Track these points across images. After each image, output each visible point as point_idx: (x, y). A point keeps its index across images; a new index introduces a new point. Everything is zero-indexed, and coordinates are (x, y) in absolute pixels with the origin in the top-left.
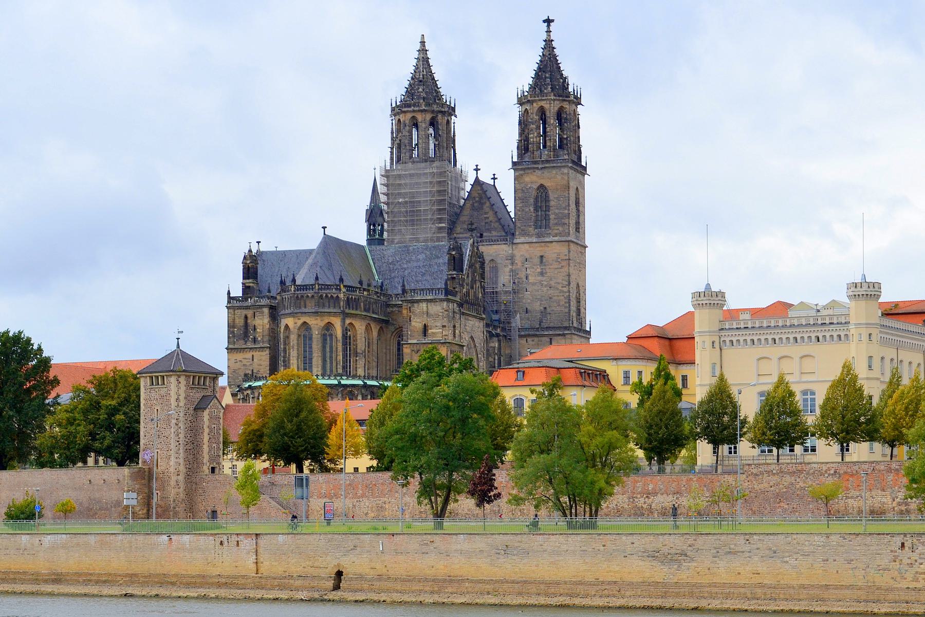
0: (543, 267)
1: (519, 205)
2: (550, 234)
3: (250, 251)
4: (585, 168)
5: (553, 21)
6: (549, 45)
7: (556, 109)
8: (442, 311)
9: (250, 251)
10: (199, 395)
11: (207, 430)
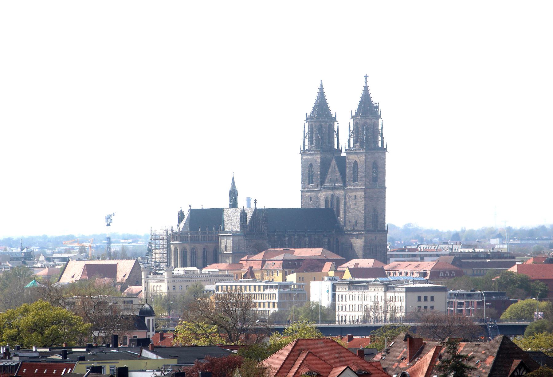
3: (181, 211)
6: (366, 89)
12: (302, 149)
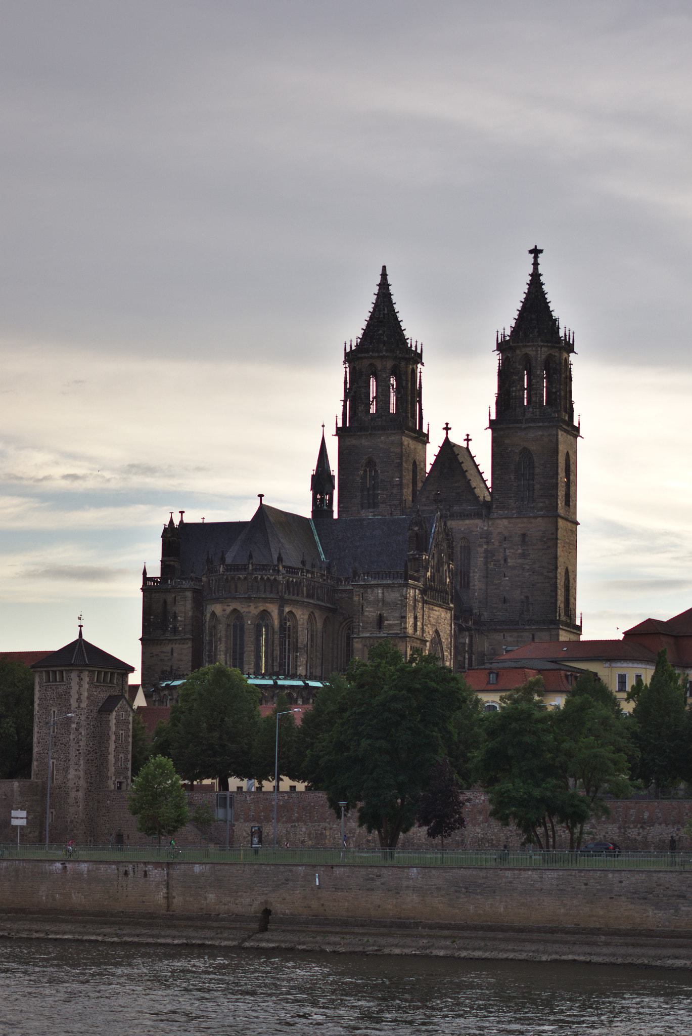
0: (526, 548)
1: (497, 472)
2: (534, 507)
3: (171, 522)
4: (577, 429)
5: (541, 251)
7: (543, 357)
8: (400, 598)
9: (171, 522)
10: (104, 695)
11: (113, 737)
12: (340, 425)
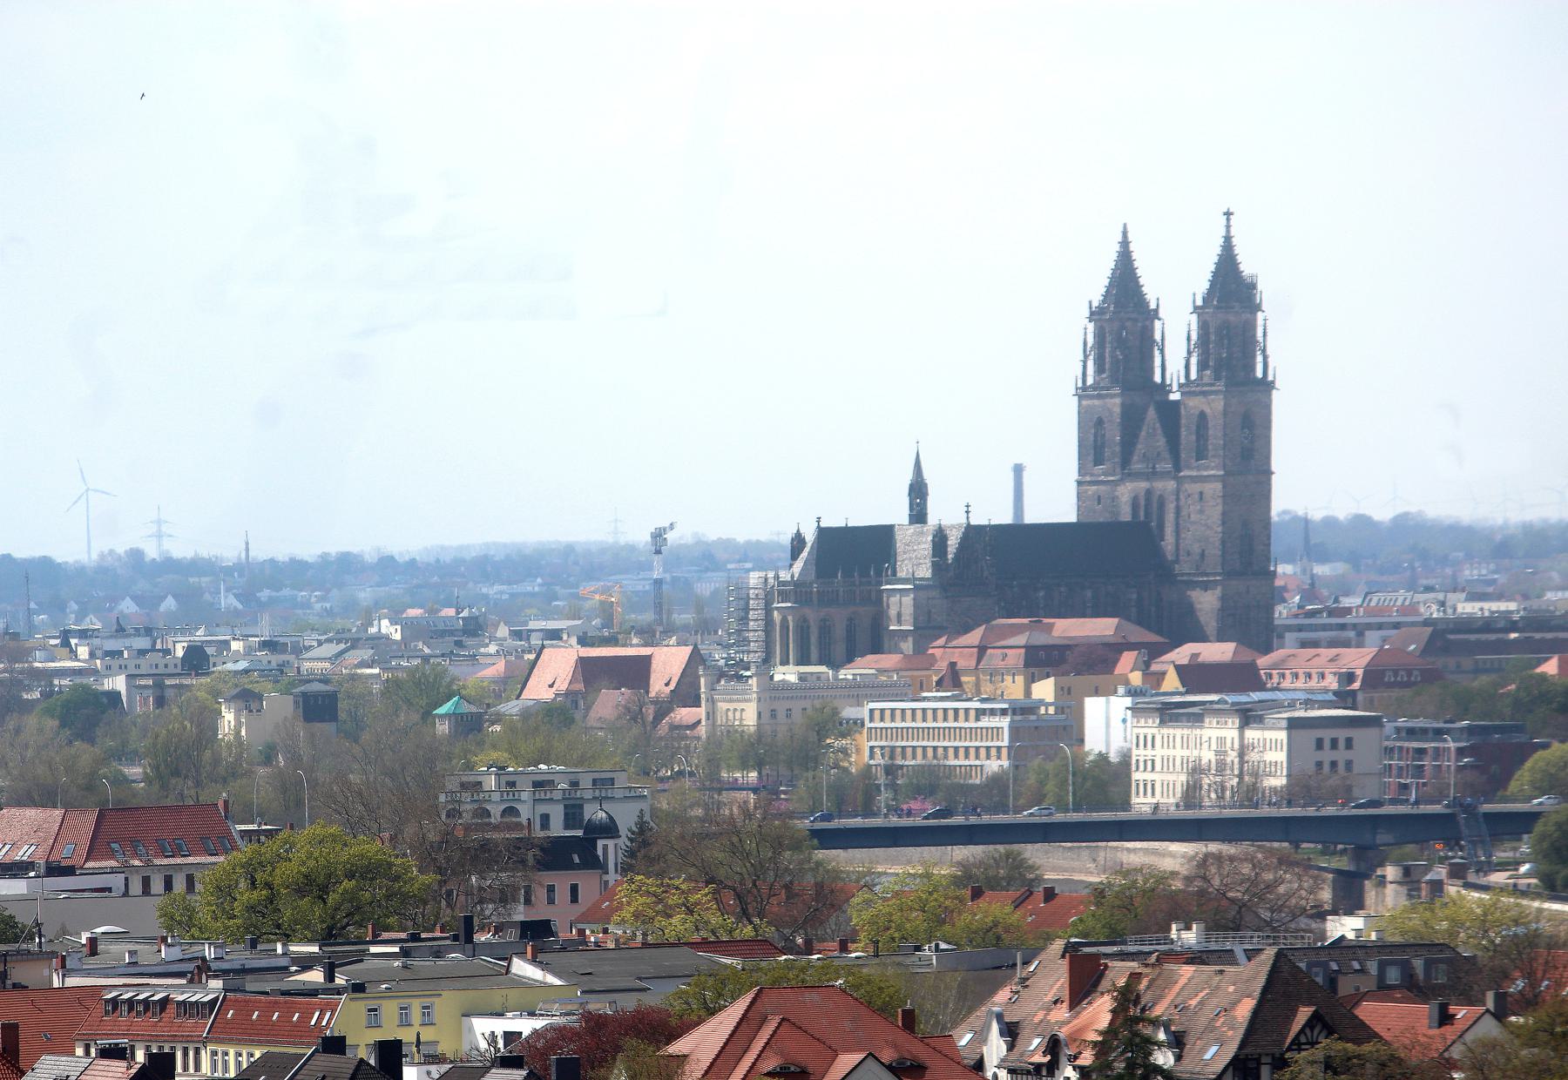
3: (798, 531)
5: (1232, 214)
12: (1080, 385)
